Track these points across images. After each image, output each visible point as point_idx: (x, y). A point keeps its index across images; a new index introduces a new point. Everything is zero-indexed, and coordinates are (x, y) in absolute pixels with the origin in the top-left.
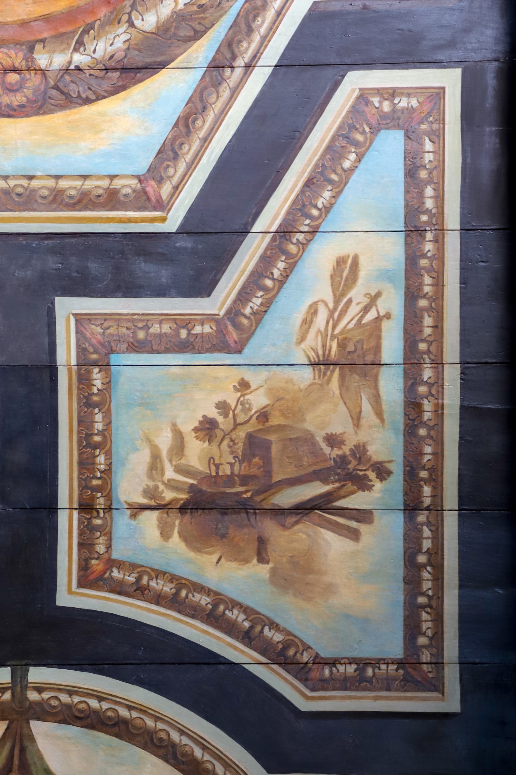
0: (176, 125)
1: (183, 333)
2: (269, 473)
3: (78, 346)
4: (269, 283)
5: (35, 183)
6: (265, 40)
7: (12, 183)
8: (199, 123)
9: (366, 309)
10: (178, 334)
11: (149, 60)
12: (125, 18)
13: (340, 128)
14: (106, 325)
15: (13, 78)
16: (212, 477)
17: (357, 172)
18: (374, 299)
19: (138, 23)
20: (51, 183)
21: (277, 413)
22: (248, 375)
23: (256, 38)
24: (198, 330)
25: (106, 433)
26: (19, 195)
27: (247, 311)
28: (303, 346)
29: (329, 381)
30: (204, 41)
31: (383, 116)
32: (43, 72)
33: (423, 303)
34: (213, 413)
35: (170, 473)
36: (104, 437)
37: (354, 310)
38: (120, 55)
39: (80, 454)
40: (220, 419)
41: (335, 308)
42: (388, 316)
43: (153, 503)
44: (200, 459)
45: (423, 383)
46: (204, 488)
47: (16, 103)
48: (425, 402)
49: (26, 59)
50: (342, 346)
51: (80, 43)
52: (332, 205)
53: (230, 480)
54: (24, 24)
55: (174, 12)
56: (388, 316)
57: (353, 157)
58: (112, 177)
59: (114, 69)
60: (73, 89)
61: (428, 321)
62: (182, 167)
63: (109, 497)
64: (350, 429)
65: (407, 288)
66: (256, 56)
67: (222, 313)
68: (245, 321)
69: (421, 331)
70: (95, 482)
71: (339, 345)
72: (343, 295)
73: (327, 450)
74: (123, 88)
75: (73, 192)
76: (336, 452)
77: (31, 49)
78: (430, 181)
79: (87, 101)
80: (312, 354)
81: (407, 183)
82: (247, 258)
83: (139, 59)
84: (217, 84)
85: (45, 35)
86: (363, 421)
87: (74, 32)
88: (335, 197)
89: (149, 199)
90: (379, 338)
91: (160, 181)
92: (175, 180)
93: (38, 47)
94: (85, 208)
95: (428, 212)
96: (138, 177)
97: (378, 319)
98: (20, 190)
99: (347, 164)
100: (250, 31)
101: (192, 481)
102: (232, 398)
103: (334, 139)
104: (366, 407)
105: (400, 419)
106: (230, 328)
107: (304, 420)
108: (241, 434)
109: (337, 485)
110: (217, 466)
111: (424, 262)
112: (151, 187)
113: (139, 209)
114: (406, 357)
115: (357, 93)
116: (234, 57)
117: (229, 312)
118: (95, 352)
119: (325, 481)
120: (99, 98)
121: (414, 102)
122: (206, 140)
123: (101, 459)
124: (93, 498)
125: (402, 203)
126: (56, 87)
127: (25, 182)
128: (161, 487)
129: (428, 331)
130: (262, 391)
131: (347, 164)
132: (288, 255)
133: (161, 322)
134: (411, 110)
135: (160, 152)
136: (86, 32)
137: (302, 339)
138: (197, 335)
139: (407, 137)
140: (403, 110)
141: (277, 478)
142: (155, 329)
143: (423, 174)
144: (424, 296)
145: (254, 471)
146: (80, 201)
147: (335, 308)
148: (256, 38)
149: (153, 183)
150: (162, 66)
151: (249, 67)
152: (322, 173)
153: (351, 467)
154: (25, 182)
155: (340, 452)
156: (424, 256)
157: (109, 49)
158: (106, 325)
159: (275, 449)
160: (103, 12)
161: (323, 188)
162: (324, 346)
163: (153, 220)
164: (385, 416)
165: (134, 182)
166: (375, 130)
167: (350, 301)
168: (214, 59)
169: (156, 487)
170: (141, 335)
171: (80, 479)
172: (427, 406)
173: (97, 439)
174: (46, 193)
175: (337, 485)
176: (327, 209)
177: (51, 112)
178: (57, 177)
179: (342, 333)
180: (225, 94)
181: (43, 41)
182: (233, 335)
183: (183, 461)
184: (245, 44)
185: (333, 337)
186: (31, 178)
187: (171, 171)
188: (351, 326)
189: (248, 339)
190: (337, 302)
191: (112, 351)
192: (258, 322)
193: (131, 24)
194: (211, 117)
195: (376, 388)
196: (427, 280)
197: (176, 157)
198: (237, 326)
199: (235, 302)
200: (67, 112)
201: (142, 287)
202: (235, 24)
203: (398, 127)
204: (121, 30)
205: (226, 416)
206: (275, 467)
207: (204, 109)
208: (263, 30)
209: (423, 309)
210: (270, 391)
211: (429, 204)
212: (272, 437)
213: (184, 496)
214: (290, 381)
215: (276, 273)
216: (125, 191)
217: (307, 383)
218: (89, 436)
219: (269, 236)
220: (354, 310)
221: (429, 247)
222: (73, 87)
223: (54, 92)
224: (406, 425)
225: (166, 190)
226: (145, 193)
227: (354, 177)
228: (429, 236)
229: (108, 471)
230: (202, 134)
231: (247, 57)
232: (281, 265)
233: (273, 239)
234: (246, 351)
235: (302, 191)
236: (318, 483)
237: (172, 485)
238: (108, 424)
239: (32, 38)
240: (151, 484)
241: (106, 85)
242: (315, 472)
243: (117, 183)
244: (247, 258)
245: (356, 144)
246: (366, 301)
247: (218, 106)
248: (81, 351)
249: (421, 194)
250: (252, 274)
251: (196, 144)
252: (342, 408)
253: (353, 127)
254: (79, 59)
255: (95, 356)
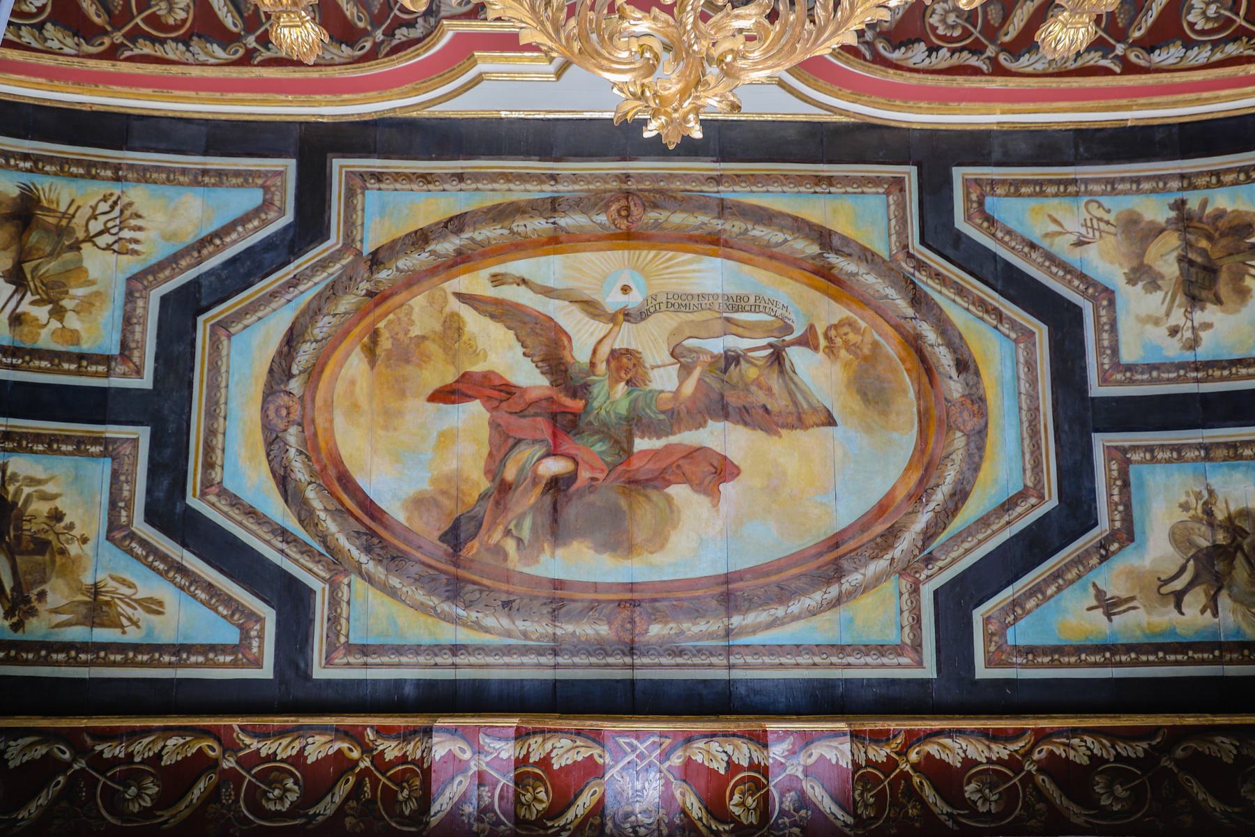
0: (251, 507)
1: (122, 504)
2: (22, 553)
3: (118, 439)
4: (151, 559)
5: (221, 420)
6: (296, 561)
7: (222, 407)
8: (251, 520)
9: (129, 619)
10: (122, 501)
11: (289, 492)
12: (313, 480)
13: (243, 606)
14: (131, 457)
15: (284, 412)
16: (23, 515)
17: (215, 615)
18: (135, 623)
19: (310, 487)
20: (221, 430)
21: (64, 560)
22: (90, 544)
23: (298, 556)
24: (124, 513)
25: (59, 452)
26: (215, 410)
27: (133, 545)
28: (109, 579)
29: (84, 594)
30: (298, 526)
31: (248, 632)
32: (285, 430)
33: (131, 655)
34: (67, 520)
35: (27, 490)
36: (56, 451)
37: (129, 611)
38: (293, 476)
39: (45, 435)
40: (62, 524)
41: (132, 600)
42: (124, 633)
43: (6, 478)
44: (36, 510)
45: (77, 654)
46: (15, 511)
47: (269, 413)
48: (64, 655)
49: (294, 421)
50: (107, 603)
51: (301, 453)
52: (196, 599)
53: (19, 528)
54: (313, 421)
55: (314, 509)
56: (124, 633)
57: (225, 612)
58: (222, 467)
59: (285, 472)
60: (275, 447)
61: (119, 658)
62: (226, 509)
63: (13, 450)
64: (49, 606)
65: (141, 645)
66: (287, 555)
67: (133, 529)
68: (127, 543)
69: (112, 653)
70: (24, 443)
71: (107, 601)
72: (140, 605)
73: (36, 591)
74: (274, 476)
75: (214, 442)
76: (34, 597)
77: (299, 424)
78: (207, 659)
79: (268, 455)
80: (102, 584)
81: (207, 645)
82: (167, 545)
83: (290, 487)
84: (273, 532)
85: (306, 433)
86: (54, 615)
87: (307, 450)
88: (202, 602)
89: (207, 487)
90: (110, 627)
91: (218, 495)
92: (218, 504)
93: (300, 429)
94: (204, 449)
95: (188, 658)
96: (220, 483)
97: (122, 627)
98: (218, 411)
99: (221, 609)
100: (302, 553)
101: (20, 504)
102: (76, 532)
103: (236, 601)
104: (64, 617)
105: (53, 639)
106: (123, 534)
107: (57, 577)
108: (51, 537)
109: (10, 597)
110: (30, 521)
111: (157, 655)
112: (214, 489)
113: (202, 482)
114: (94, 644)
115: (262, 615)
116: (288, 543)
117: (133, 533)
118: (114, 449)
119: (13, 590)
120: (270, 462)
121: (255, 650)
122: (240, 524)
123: (41, 448)
124: (13, 441)
125: (194, 642)
126: (277, 437)
127: (222, 414)
128: (17, 484)
129: (112, 657)
130: (80, 552)
131: (221, 609)
132: (167, 572)
133: (130, 491)
134: (250, 648)
135: (235, 496)
136: (307, 456)
137: (113, 578)
138: (120, 512)
139: (235, 646)
140: (250, 644)
141: (18, 559)
142: (126, 487)
143: (211, 656)
144: (135, 656)
145: (24, 544)
146: (209, 446)
147: (132, 600)
148: (298, 556)
149: (217, 490)
150: (286, 501)
151: (282, 551)
152: (216, 593)
153: (22, 606)
154: (222, 414)
155: (33, 600)
156: (161, 656)
157: (296, 470)
158: (131, 457)
159: (39, 558)
160: (317, 467)
161: (207, 594)
162: (107, 592)
163: (194, 489)
164: (56, 630)
165: (218, 479)
166: (241, 627)
167: (135, 609)
168: (287, 531)
169: (18, 481)
170: (123, 478)
171: (27, 433)
172: (61, 657)
173: (55, 446)
174: (215, 426)
175: (10, 597)
176: (194, 596)
177: (263, 433)
178: (224, 434)
179: (115, 603)
180: (267, 537)
181: (303, 431)
182: (118, 535)
183: (35, 499)
184: (295, 549)
185: (113, 598)
186: (225, 418)
187: (223, 502)
188: (119, 609)
189: (115, 544)
190: (136, 601)
191: (113, 459)
192: (126, 551)
193: (309, 483)
194: (254, 527)
195: (76, 624)
196: (145, 658)
197: (232, 505)
198: (124, 538)
199: (140, 537)
200: (263, 443)
201: (153, 480)
202: (306, 544)
203: (241, 640)
204: (306, 477)
205: (64, 528)
206: (26, 558)
207: (259, 524)
208: (302, 561)
209: (127, 655)
210: (79, 557)
211: (193, 659)
212: (47, 557)
213: (10, 498)
214: (85, 569)
215: (156, 564)
216: (213, 473)
217: (83, 580)
218: (57, 441)
219: (179, 559)
220: (129, 611)
221: (166, 658)
222: (277, 447)
223: (274, 435)
224: (50, 642)
225: (213, 498)
226: (212, 486)
227: (212, 613)
228: (173, 659)
229: (32, 451)
230: (245, 522)
231: (287, 551)
232: (161, 567)
233: (178, 563)
234: (108, 543)
235: (206, 581)
236: (12, 584)
237: (18, 492)
238: (64, 454)
239: (305, 425)
240: (21, 478)
241: (276, 466)
242: (20, 583)
243: (218, 469)
244: (167, 545)
245: (233, 615)
246: (135, 619)
247: (260, 532)
248: (115, 441)
249: (199, 653)
250: (157, 549)
251: (239, 518)
252: (64, 602)
253: (242, 612)
254: (292, 452)
255: (111, 448)
